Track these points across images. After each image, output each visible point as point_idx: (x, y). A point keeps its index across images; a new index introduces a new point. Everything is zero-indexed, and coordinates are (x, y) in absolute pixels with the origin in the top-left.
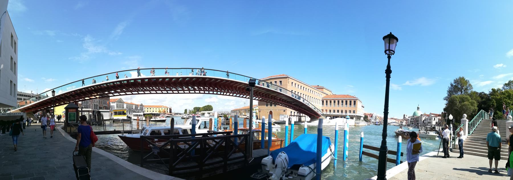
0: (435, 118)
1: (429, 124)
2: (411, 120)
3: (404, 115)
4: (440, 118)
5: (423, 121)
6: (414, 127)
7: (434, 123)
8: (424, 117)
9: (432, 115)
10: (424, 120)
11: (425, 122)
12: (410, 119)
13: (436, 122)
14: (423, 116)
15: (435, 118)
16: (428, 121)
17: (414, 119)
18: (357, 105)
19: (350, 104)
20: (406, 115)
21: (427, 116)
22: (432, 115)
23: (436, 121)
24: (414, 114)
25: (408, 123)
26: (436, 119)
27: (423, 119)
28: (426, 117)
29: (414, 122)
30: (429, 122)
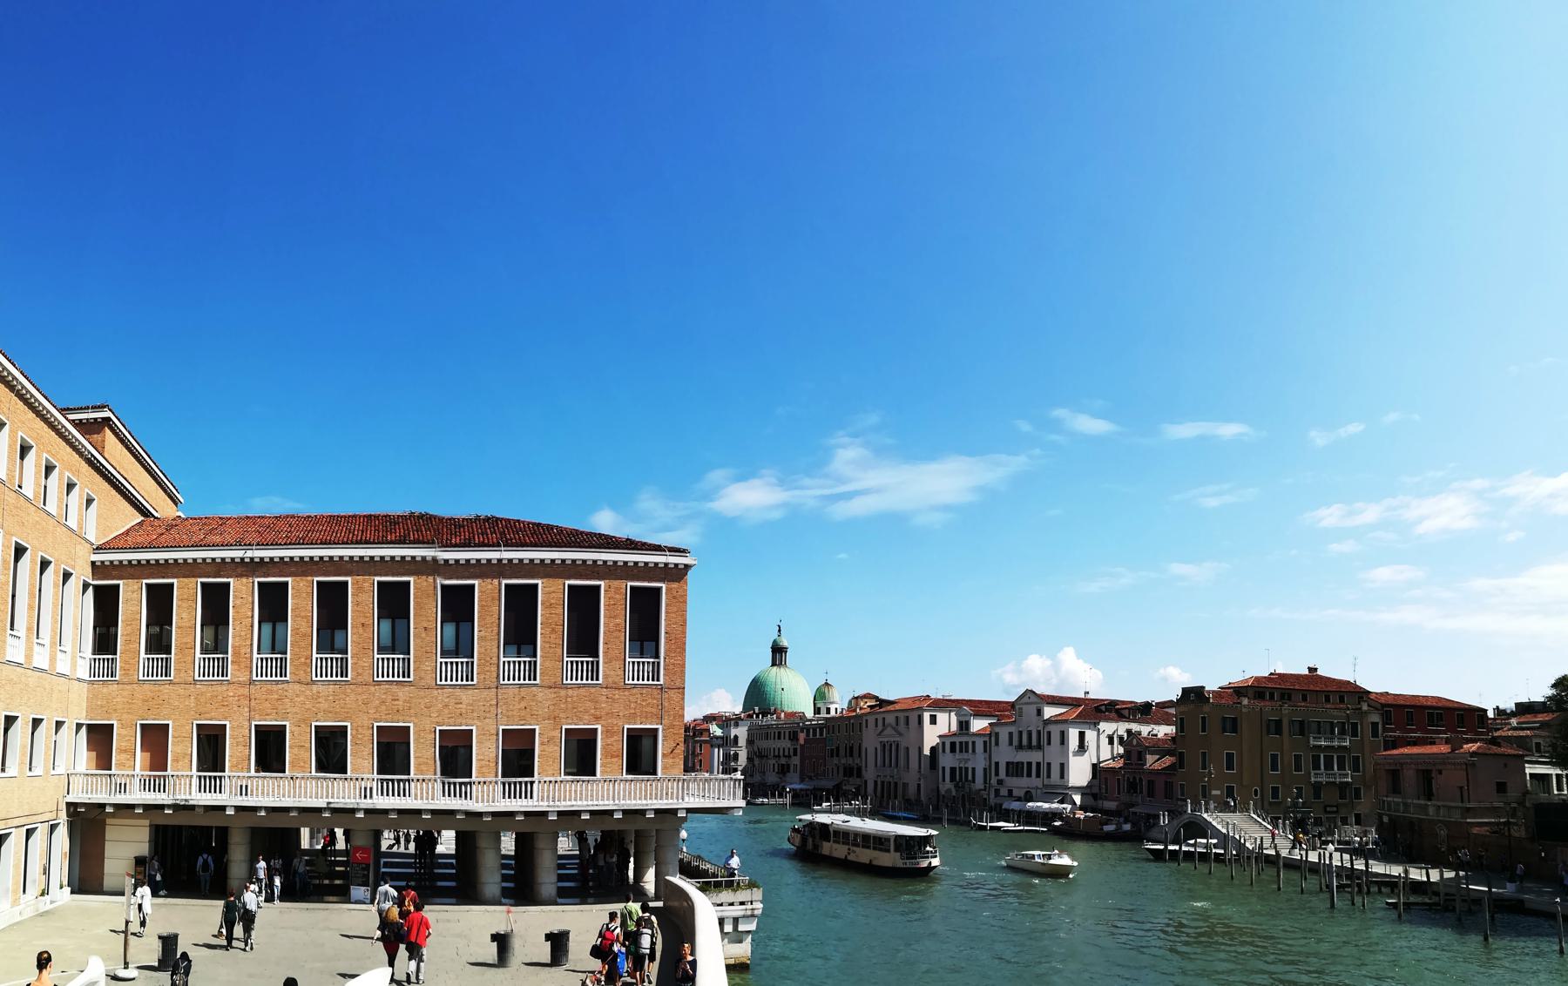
0: (1082, 735)
1: (1020, 784)
2: (763, 744)
5: (927, 752)
6: (794, 784)
8: (933, 720)
9: (1050, 712)
10: (933, 749)
11: (947, 761)
12: (741, 732)
14: (927, 716)
15: (1082, 735)
16: (1005, 754)
17: (794, 737)
18: (679, 646)
19: (583, 639)
24: (757, 695)
26: (1090, 735)
27: (931, 736)
28: (964, 726)
29: (796, 760)
30: (1015, 769)
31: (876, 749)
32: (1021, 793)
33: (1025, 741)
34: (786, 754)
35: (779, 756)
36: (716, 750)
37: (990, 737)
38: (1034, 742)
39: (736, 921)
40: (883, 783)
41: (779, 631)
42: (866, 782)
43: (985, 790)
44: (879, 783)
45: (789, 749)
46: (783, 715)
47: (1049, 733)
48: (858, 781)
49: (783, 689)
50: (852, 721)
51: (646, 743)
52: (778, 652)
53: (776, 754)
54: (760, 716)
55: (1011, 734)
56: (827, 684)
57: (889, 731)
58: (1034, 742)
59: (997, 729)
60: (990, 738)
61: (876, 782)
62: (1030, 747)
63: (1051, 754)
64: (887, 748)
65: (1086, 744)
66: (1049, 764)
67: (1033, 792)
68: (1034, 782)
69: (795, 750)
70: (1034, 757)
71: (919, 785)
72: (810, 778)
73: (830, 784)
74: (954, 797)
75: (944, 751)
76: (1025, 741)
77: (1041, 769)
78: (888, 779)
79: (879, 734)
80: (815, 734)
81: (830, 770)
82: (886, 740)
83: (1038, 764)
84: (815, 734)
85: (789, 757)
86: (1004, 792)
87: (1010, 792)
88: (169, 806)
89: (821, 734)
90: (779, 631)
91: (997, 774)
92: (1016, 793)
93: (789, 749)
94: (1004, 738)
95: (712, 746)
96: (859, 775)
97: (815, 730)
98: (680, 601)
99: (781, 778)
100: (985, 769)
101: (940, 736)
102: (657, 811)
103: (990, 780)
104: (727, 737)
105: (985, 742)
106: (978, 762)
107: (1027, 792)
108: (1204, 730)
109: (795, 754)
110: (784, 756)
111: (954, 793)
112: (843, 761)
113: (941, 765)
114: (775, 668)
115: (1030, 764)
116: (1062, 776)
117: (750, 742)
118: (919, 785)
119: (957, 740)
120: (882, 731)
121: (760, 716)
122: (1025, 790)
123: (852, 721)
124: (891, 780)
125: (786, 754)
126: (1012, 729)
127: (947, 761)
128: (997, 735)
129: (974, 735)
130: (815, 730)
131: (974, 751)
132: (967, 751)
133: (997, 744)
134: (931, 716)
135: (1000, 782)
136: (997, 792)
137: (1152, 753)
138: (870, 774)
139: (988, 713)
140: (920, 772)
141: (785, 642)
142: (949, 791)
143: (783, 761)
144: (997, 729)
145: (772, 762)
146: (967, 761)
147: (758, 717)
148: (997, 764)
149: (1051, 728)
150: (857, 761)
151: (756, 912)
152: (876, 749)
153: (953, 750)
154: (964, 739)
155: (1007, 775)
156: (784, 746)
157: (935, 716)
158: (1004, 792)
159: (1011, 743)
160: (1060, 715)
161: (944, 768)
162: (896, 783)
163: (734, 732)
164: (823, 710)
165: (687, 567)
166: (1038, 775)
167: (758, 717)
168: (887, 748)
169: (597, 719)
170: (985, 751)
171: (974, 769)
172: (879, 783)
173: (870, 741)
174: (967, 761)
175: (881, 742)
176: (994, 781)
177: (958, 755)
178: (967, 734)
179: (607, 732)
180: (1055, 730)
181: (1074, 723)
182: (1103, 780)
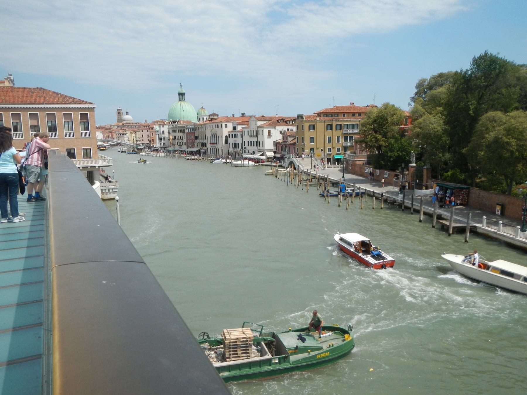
0: (269, 132)
3: (119, 113)
4: (285, 128)
7: (269, 144)
8: (226, 126)
9: (260, 123)
11: (231, 141)
12: (166, 129)
13: (274, 142)
15: (269, 132)
16: (247, 138)
20: (124, 111)
21: (239, 124)
22: (260, 123)
23: (273, 139)
25: (163, 142)
26: (273, 131)
27: (226, 131)
28: (235, 128)
29: (185, 141)
31: (210, 136)
32: (251, 152)
33: (252, 134)
34: (181, 138)
35: (179, 139)
36: (157, 136)
37: (242, 133)
38: (255, 135)
39: (112, 189)
41: (181, 86)
42: (208, 148)
43: (241, 151)
44: (212, 149)
45: (182, 136)
46: (182, 122)
47: (259, 131)
48: (206, 148)
49: (183, 111)
50: (203, 126)
51: (88, 151)
52: (181, 95)
53: (178, 138)
54: (173, 123)
55: (248, 131)
56: (202, 108)
57: (213, 131)
58: (255, 135)
59: (243, 130)
60: (242, 133)
61: (211, 149)
62: (254, 136)
63: (260, 138)
64: (214, 136)
65: (271, 134)
66: (259, 142)
67: (255, 151)
68: (255, 148)
69: (184, 137)
70: (254, 139)
71: (222, 149)
72: (190, 147)
73: (194, 150)
74: (233, 153)
75: (229, 137)
76: (252, 134)
77: (257, 144)
78: (214, 148)
79: (211, 131)
80: (191, 131)
81: (197, 144)
82: (213, 133)
83: (256, 142)
84: (191, 131)
86: (247, 151)
87: (249, 151)
89: (193, 131)
90: (181, 86)
91: (245, 145)
92: (250, 152)
93: (182, 136)
94: (246, 133)
96: (206, 146)
98: (93, 117)
99: (180, 147)
100: (241, 143)
101: (229, 132)
102: (91, 167)
103: (243, 147)
105: (241, 134)
106: (239, 141)
107: (253, 151)
108: (303, 130)
110: (177, 139)
111: (233, 152)
112: (200, 141)
113: (229, 142)
114: (180, 103)
115: (254, 142)
116: (263, 146)
117: (169, 133)
118: (222, 149)
119: (233, 133)
120: (212, 130)
121: (173, 123)
122: (253, 151)
123: (203, 126)
124: (215, 148)
125: (181, 138)
126: (249, 130)
127: (231, 141)
128: (244, 131)
129: (238, 131)
131: (238, 137)
132: (236, 137)
133: (244, 135)
134: (225, 124)
135: (245, 148)
136: (245, 151)
137: (291, 137)
138: (209, 146)
139: (244, 123)
141: (184, 91)
142: (231, 151)
143: (180, 141)
144: (243, 130)
145: (177, 141)
146: (236, 141)
147: (172, 123)
148: (244, 142)
149: (259, 129)
150: (205, 141)
151: (117, 187)
152: (210, 136)
153: (232, 137)
154: (235, 133)
155: (248, 145)
156: (180, 135)
157: (227, 124)
158: (247, 151)
159: (248, 135)
160: (263, 124)
161: (230, 143)
162: (217, 149)
163: (162, 129)
164: (201, 119)
165: (94, 108)
166: (256, 146)
167: (172, 123)
168: (214, 136)
169: (75, 146)
170: (241, 137)
171: (238, 144)
172: (212, 149)
173: (208, 134)
174: (236, 141)
176: (243, 148)
177: (234, 139)
178: (236, 131)
179: (77, 149)
180: (260, 130)
181: (266, 127)
182: (277, 146)
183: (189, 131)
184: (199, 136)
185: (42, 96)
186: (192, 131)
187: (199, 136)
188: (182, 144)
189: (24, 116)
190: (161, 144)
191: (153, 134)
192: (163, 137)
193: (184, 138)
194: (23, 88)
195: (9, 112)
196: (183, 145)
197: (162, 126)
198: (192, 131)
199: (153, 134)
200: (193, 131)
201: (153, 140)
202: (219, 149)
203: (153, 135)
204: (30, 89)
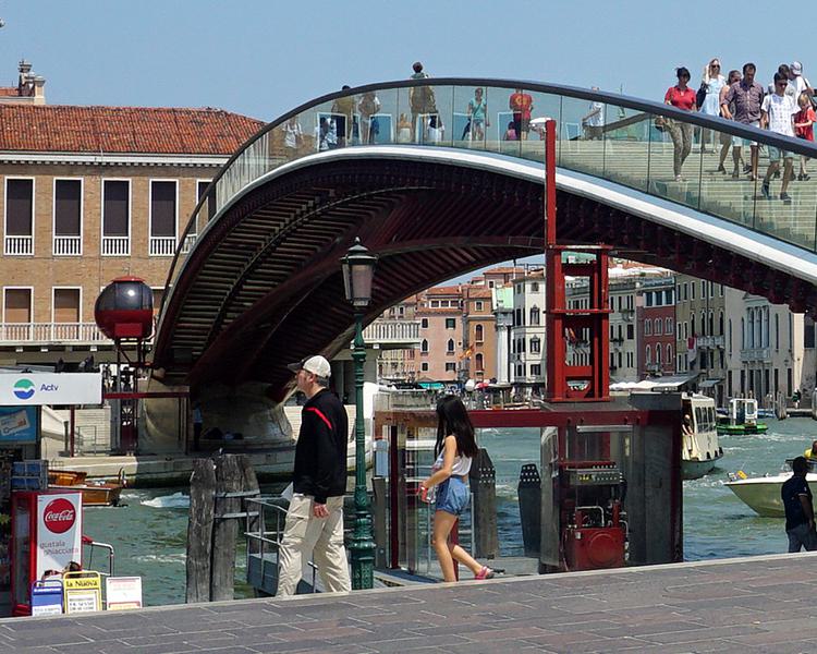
34: (616, 336)
36: (504, 334)
40: (752, 371)
42: (730, 372)
61: (743, 372)
69: (630, 328)
80: (659, 301)
84: (659, 301)
85: (621, 340)
88: (45, 347)
89: (669, 301)
95: (497, 328)
97: (659, 294)
104: (519, 311)
109: (630, 336)
125: (616, 336)
130: (659, 294)
138: (734, 363)
140: (790, 351)
150: (719, 341)
162: (767, 371)
168: (756, 318)
175: (749, 309)
183: (649, 301)
184: (693, 322)
185: (229, 135)
186: (664, 304)
187: (693, 322)
188: (616, 363)
189: (185, 189)
190: (520, 370)
191: (479, 328)
192: (532, 336)
193: (630, 336)
194: (168, 111)
195: (146, 179)
196: (620, 366)
197: (528, 287)
198: (664, 304)
199: (479, 328)
200: (669, 301)
201: (479, 357)
202: (776, 371)
203: (479, 336)
204: (188, 112)
